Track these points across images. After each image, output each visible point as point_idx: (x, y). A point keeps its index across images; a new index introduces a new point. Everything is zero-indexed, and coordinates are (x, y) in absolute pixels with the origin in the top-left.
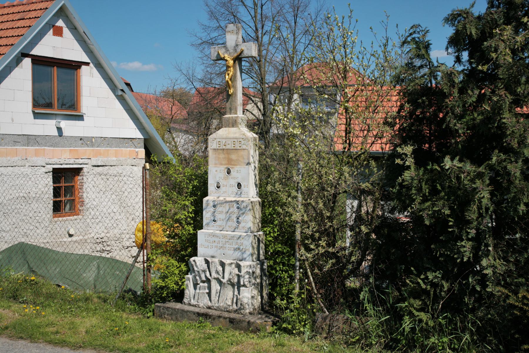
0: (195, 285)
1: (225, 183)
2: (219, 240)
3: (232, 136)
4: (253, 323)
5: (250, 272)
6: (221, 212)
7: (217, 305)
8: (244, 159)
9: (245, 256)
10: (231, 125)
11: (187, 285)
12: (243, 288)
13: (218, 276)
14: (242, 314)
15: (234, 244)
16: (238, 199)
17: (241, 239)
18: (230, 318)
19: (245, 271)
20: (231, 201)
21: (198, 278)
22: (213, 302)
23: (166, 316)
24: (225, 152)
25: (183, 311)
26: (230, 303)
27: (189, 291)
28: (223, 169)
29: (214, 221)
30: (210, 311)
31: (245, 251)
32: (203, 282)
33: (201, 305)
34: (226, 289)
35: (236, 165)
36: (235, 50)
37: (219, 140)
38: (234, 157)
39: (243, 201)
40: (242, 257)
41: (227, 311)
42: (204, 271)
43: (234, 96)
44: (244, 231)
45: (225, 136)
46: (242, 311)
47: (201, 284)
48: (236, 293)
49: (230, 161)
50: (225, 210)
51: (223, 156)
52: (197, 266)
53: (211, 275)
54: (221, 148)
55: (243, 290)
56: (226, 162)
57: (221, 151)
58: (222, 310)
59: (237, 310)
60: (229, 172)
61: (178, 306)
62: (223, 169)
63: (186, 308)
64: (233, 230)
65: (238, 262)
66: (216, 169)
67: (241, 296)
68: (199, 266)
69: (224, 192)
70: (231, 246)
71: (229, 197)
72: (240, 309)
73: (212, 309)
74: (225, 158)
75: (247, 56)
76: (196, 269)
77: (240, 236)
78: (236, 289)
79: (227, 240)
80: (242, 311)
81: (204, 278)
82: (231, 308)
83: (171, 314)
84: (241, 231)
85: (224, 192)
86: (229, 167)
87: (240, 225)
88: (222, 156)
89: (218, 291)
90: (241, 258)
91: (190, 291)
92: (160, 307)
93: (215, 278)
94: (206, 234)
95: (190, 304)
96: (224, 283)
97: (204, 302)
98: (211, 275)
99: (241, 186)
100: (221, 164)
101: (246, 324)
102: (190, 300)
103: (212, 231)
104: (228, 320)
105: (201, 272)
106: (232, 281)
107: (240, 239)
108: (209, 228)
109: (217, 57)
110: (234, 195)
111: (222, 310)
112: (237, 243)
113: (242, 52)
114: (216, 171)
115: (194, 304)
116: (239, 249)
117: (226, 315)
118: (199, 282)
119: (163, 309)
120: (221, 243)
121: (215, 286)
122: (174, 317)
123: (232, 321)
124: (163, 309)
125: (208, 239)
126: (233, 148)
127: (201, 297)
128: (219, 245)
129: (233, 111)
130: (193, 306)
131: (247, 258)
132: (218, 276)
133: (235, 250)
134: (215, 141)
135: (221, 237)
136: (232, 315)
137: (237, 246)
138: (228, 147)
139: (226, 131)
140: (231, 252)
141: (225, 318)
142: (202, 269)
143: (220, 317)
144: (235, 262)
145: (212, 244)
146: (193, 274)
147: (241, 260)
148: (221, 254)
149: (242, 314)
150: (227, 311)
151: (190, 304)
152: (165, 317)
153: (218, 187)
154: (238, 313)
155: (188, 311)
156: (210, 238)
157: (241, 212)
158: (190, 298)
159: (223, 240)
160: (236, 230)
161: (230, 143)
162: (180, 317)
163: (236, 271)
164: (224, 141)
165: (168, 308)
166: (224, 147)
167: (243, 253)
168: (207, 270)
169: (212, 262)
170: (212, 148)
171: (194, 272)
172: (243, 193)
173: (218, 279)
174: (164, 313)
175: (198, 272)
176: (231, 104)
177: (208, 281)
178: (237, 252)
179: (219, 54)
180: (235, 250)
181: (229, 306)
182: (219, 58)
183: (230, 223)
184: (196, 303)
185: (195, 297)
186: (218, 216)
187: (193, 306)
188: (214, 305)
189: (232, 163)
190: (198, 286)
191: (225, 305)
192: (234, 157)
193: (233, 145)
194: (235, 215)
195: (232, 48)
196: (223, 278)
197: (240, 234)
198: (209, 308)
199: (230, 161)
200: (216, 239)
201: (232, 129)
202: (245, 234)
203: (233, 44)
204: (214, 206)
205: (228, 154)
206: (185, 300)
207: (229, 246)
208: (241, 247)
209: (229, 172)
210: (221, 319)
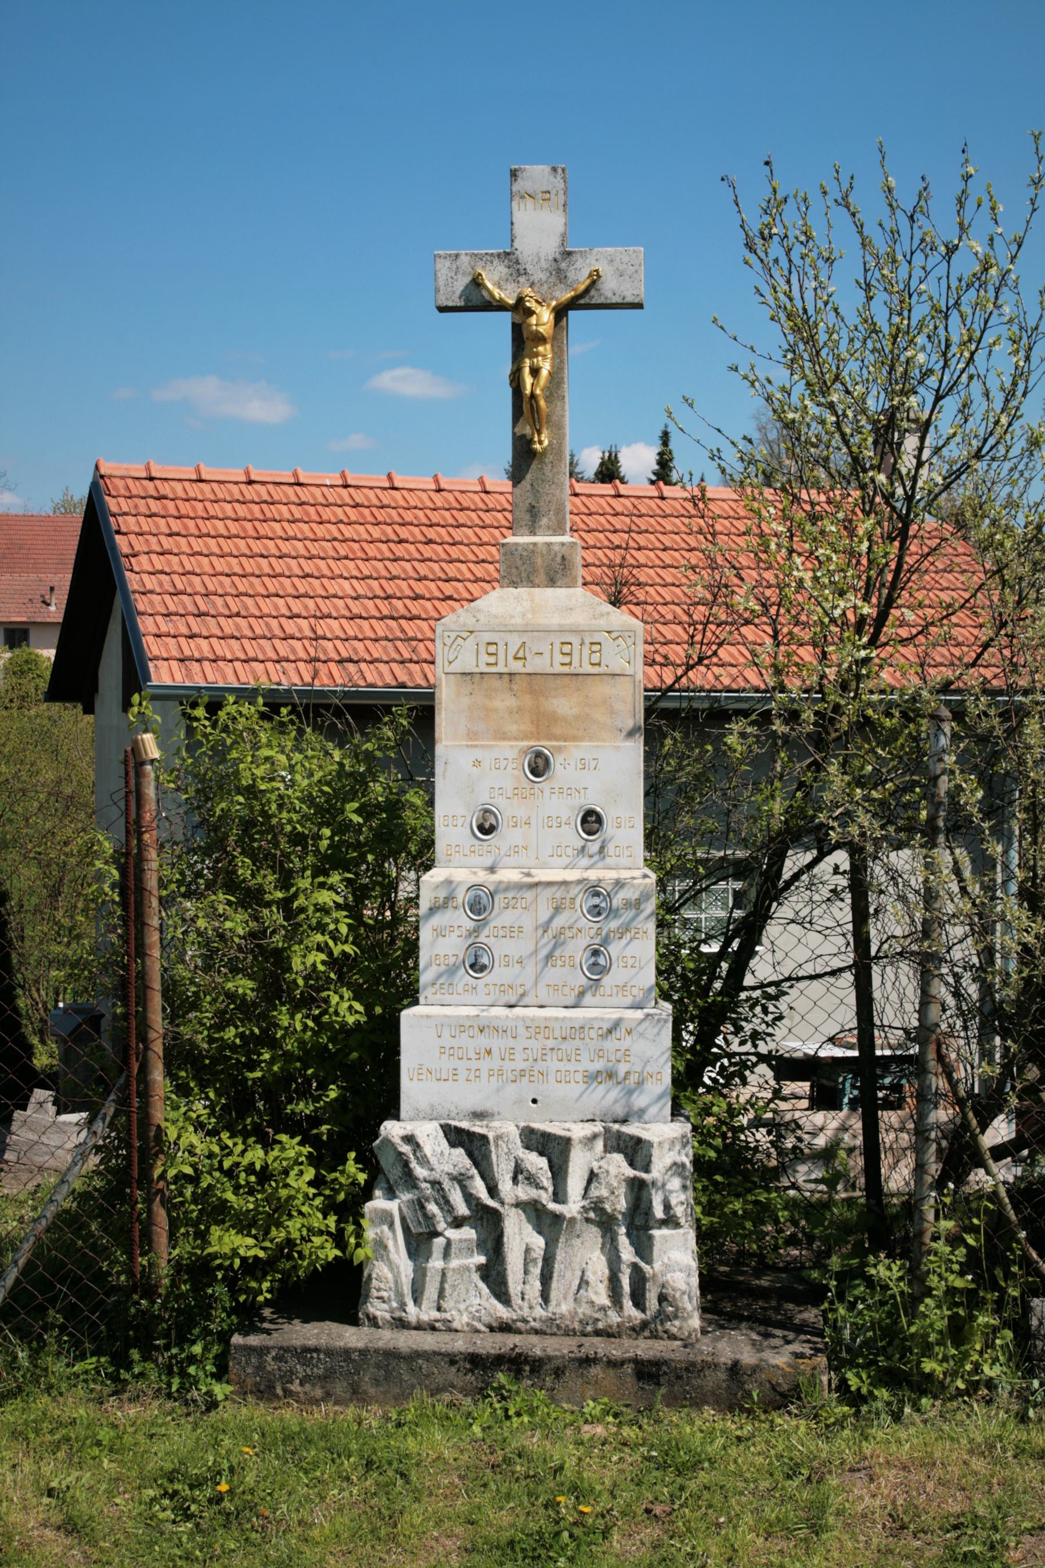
0: (419, 1243)
1: (521, 813)
2: (511, 1043)
3: (555, 620)
4: (755, 1369)
5: (683, 1165)
6: (512, 932)
7: (539, 1312)
8: (612, 712)
9: (640, 1101)
10: (542, 577)
11: (381, 1245)
12: (665, 1232)
13: (533, 1193)
14: (673, 1337)
15: (585, 1057)
16: (593, 875)
17: (620, 1032)
18: (636, 1361)
19: (668, 1161)
20: (565, 883)
21: (432, 1208)
22: (516, 1300)
23: (295, 1387)
24: (519, 684)
25: (391, 1355)
26: (601, 1296)
27: (391, 1265)
28: (511, 754)
29: (477, 967)
30: (510, 1341)
31: (640, 1084)
32: (458, 1223)
33: (460, 1321)
34: (577, 1242)
35: (575, 739)
36: (560, 276)
37: (488, 637)
38: (564, 705)
39: (619, 884)
40: (628, 1105)
41: (598, 1333)
42: (461, 1180)
43: (550, 458)
44: (629, 1000)
45: (518, 621)
46: (674, 1326)
47: (452, 1234)
48: (627, 1253)
49: (544, 723)
50: (528, 922)
51: (511, 702)
52: (424, 1161)
53: (493, 1190)
54: (501, 668)
55: (663, 1237)
56: (526, 727)
57: (497, 683)
58: (569, 1332)
59: (645, 1324)
60: (539, 766)
61: (351, 1337)
62: (511, 754)
63: (388, 1338)
64: (570, 1001)
65: (616, 1127)
66: (478, 754)
67: (657, 1265)
68: (433, 1160)
69: (515, 850)
70: (571, 1067)
71: (544, 866)
72: (661, 1316)
73: (519, 1332)
74: (520, 709)
75: (615, 300)
76: (420, 1172)
77: (617, 1024)
78: (623, 1241)
79: (550, 1043)
80: (674, 1326)
81: (462, 1209)
82: (614, 1318)
83: (326, 1378)
84: (609, 1001)
85: (515, 850)
86: (545, 746)
87: (607, 980)
88: (504, 701)
89: (538, 1253)
90: (620, 1111)
91: (390, 1269)
92: (261, 1351)
93: (518, 1205)
94: (440, 1025)
95: (401, 1324)
96: (572, 1220)
97: (470, 1305)
98: (493, 1190)
99: (599, 820)
100: (504, 737)
101: (722, 1375)
102: (403, 1306)
103: (472, 1011)
104: (629, 1369)
105: (447, 1184)
106: (608, 1207)
107: (617, 1034)
108: (448, 998)
109: (465, 294)
110: (565, 860)
111: (569, 1332)
112: (600, 1053)
113: (595, 280)
114: (477, 763)
115: (425, 1317)
116: (611, 1075)
117: (615, 1350)
118: (441, 1226)
119: (277, 1358)
120: (519, 1056)
121: (520, 1236)
122: (340, 1388)
123: (648, 1372)
124: (277, 1358)
125: (455, 1043)
126: (558, 669)
127: (454, 1287)
128: (508, 1065)
129: (544, 521)
130: (419, 1327)
131: (653, 1110)
132: (533, 1193)
133: (593, 1078)
135: (521, 1030)
136: (645, 1348)
137: (599, 1065)
138: (535, 665)
139: (517, 598)
140: (574, 1089)
141: (613, 1364)
142: (448, 1168)
143: (587, 1361)
144: (598, 1127)
145: (474, 1064)
146: (406, 1196)
147: (624, 1121)
148: (519, 1102)
149: (673, 1337)
150: (598, 1333)
151: (401, 1324)
152: (288, 1393)
153: (487, 830)
154: (654, 1336)
155: (417, 1355)
156: (463, 1040)
157: (614, 924)
158: (399, 1294)
159: (530, 1043)
160: (588, 999)
161: (546, 649)
162: (376, 1382)
163: (618, 1166)
164: (515, 642)
165: (307, 1350)
166: (516, 666)
167: (630, 1092)
168: (474, 1171)
169: (498, 1138)
170: (456, 667)
171: (415, 1187)
172: (611, 849)
173: (535, 1212)
174: (288, 1377)
175: (436, 1184)
176: (535, 491)
177: (488, 1222)
178: (602, 1088)
179: (477, 283)
180: (593, 1078)
181: (603, 1309)
182: (475, 302)
183: (554, 974)
184: (435, 1315)
185: (427, 1292)
186: (499, 947)
187: (419, 1327)
188: (526, 1312)
189: (557, 731)
190: (439, 1242)
191: (584, 1310)
192: (564, 705)
193: (559, 658)
194: (583, 941)
195: (544, 264)
196: (559, 1196)
197: (614, 1014)
198: (505, 1328)
199: (544, 723)
200: (497, 1043)
201: (550, 592)
202: (639, 1014)
203: (550, 247)
204: (477, 907)
205: (533, 693)
206: (377, 1309)
207: (561, 1066)
208: (622, 1069)
209: (539, 766)
210: (595, 1371)
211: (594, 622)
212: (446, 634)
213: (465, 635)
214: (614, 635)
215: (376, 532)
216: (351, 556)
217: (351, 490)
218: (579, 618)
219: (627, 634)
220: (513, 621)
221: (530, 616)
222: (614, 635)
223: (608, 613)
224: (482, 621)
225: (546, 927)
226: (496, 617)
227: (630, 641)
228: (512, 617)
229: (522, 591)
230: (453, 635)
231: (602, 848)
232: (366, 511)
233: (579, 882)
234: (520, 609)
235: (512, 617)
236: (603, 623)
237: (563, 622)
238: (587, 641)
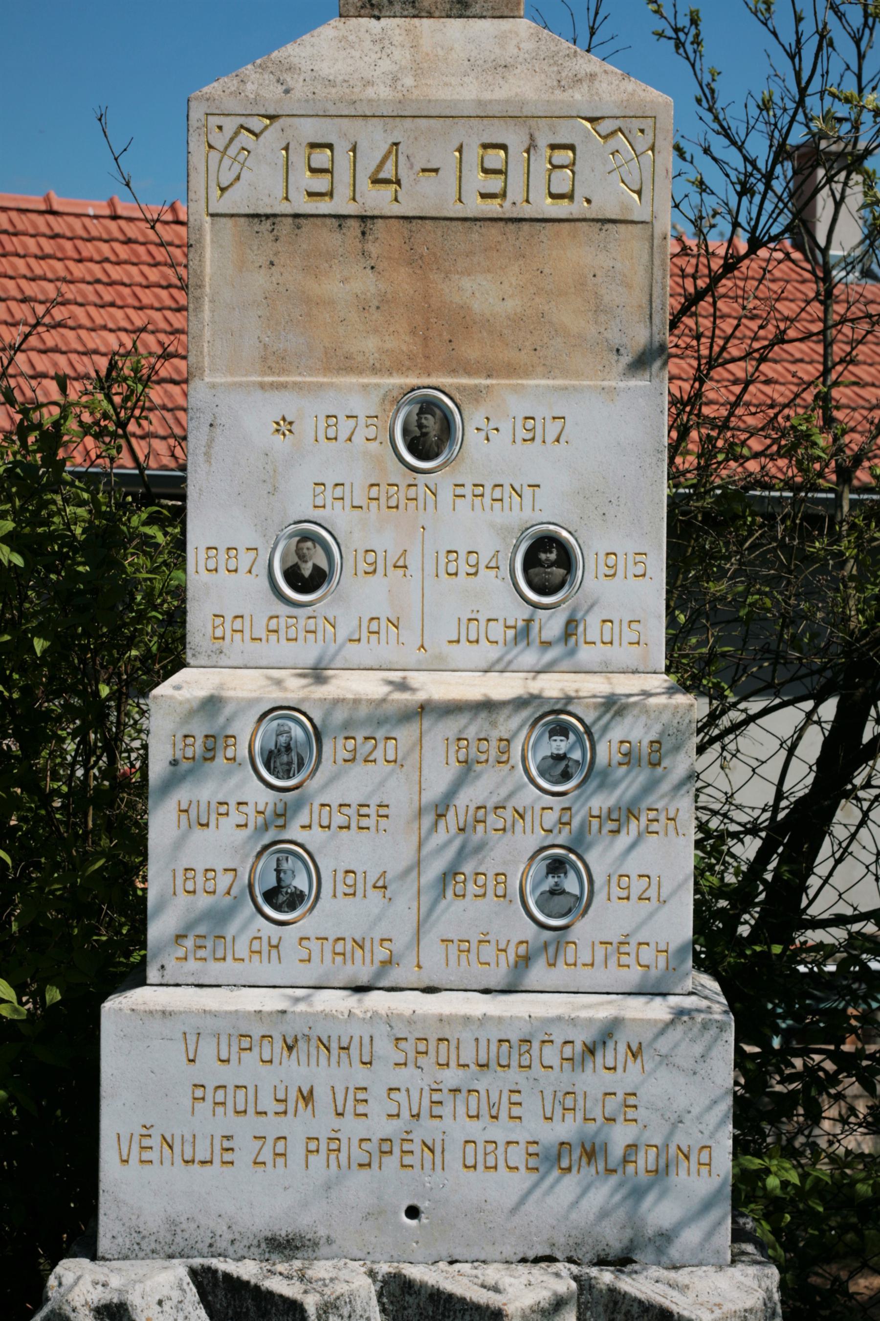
1: (386, 542)
3: (467, 92)
6: (363, 816)
8: (599, 309)
9: (660, 1213)
15: (531, 1107)
16: (552, 686)
20: (488, 706)
24: (383, 241)
28: (362, 405)
31: (661, 1172)
35: (511, 370)
37: (310, 130)
39: (613, 706)
40: (633, 1221)
44: (633, 976)
45: (382, 92)
49: (441, 333)
50: (400, 795)
51: (365, 283)
54: (340, 205)
56: (400, 342)
57: (329, 238)
60: (429, 435)
62: (362, 404)
64: (497, 976)
65: (606, 1277)
66: (285, 404)
69: (373, 627)
70: (499, 1132)
71: (438, 666)
74: (384, 302)
77: (609, 1032)
79: (451, 1077)
84: (585, 977)
85: (373, 627)
87: (584, 930)
88: (347, 283)
90: (613, 1238)
94: (194, 1033)
100: (347, 364)
103: (270, 1001)
108: (214, 971)
110: (488, 653)
112: (566, 1101)
114: (285, 426)
116: (591, 1152)
120: (378, 1107)
125: (228, 1075)
126: (476, 206)
128: (352, 1128)
131: (691, 1236)
133: (553, 1159)
134: (272, 136)
135: (384, 1047)
137: (565, 1129)
138: (422, 196)
140: (506, 1186)
145: (272, 1126)
147: (622, 1262)
148: (375, 1214)
153: (306, 579)
156: (248, 1069)
157: (600, 802)
159: (405, 1077)
161: (447, 160)
164: (374, 142)
166: (378, 200)
167: (638, 1193)
170: (237, 200)
172: (592, 627)
180: (553, 1159)
183: (459, 915)
189: (471, 352)
192: (485, 291)
193: (477, 181)
197: (602, 1009)
199: (441, 333)
200: (324, 1076)
202: (658, 1010)
204: (281, 759)
205: (416, 261)
207: (474, 1129)
208: (620, 1136)
209: (429, 435)
211: (559, 95)
212: (214, 121)
213: (257, 124)
214: (606, 126)
215: (154, 275)
216: (119, 302)
217: (122, 223)
218: (525, 88)
219: (636, 124)
220: (370, 92)
221: (409, 81)
222: (606, 126)
223: (592, 76)
224: (297, 94)
225: (441, 809)
226: (331, 83)
227: (642, 142)
228: (368, 83)
229: (392, 26)
230: (229, 125)
231: (571, 628)
232: (141, 250)
233: (520, 703)
234: (386, 65)
235: (368, 83)
236: (579, 98)
237: (487, 96)
238: (543, 142)
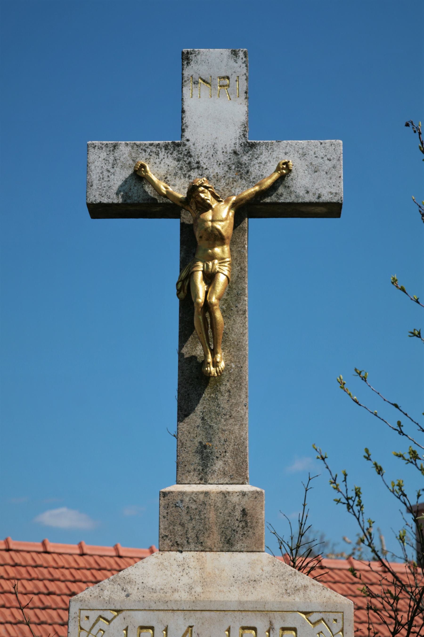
3: (233, 596)
10: (215, 538)
36: (241, 171)
37: (141, 618)
45: (183, 596)
113: (285, 173)
129: (219, 465)
134: (118, 623)
179: (139, 176)
201: (225, 557)
203: (229, 136)
211: (286, 599)
212: (84, 613)
213: (109, 615)
214: (314, 617)
215: (30, 586)
216: (8, 605)
217: (12, 553)
218: (267, 594)
219: (332, 616)
220: (176, 596)
221: (199, 589)
222: (314, 617)
223: (305, 587)
224: (133, 597)
226: (154, 590)
227: (336, 627)
228: (175, 590)
229: (189, 556)
230: (94, 615)
232: (23, 570)
234: (185, 580)
235: (175, 590)
236: (298, 599)
237: (244, 598)
238: (277, 626)
